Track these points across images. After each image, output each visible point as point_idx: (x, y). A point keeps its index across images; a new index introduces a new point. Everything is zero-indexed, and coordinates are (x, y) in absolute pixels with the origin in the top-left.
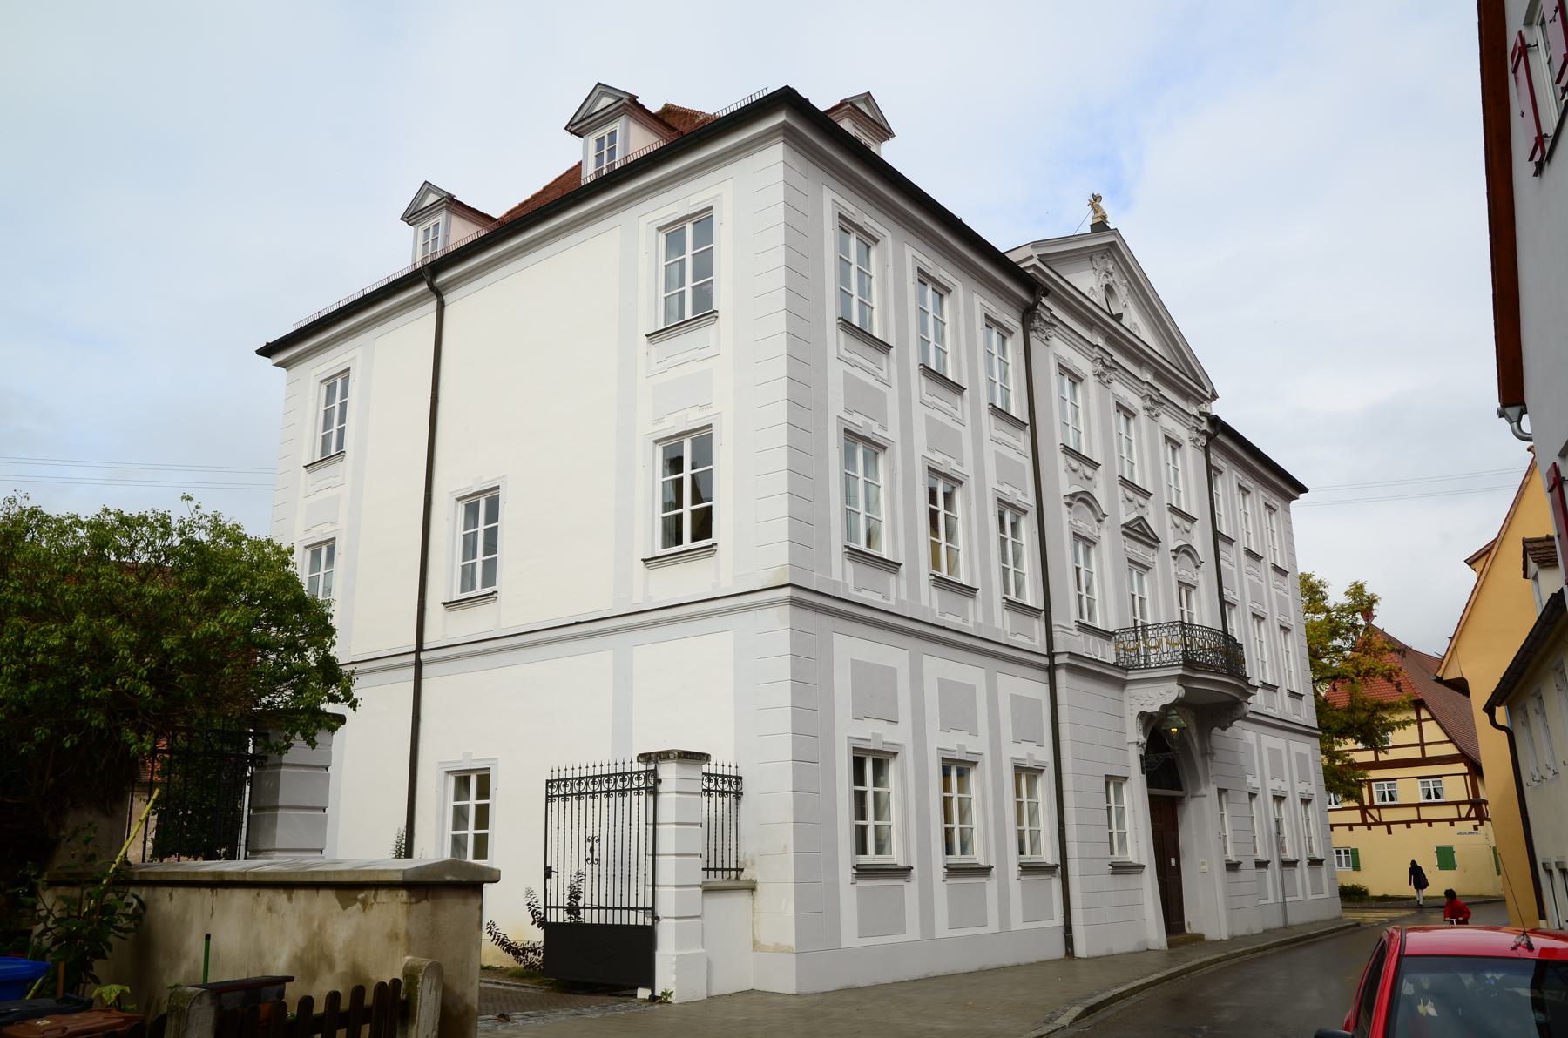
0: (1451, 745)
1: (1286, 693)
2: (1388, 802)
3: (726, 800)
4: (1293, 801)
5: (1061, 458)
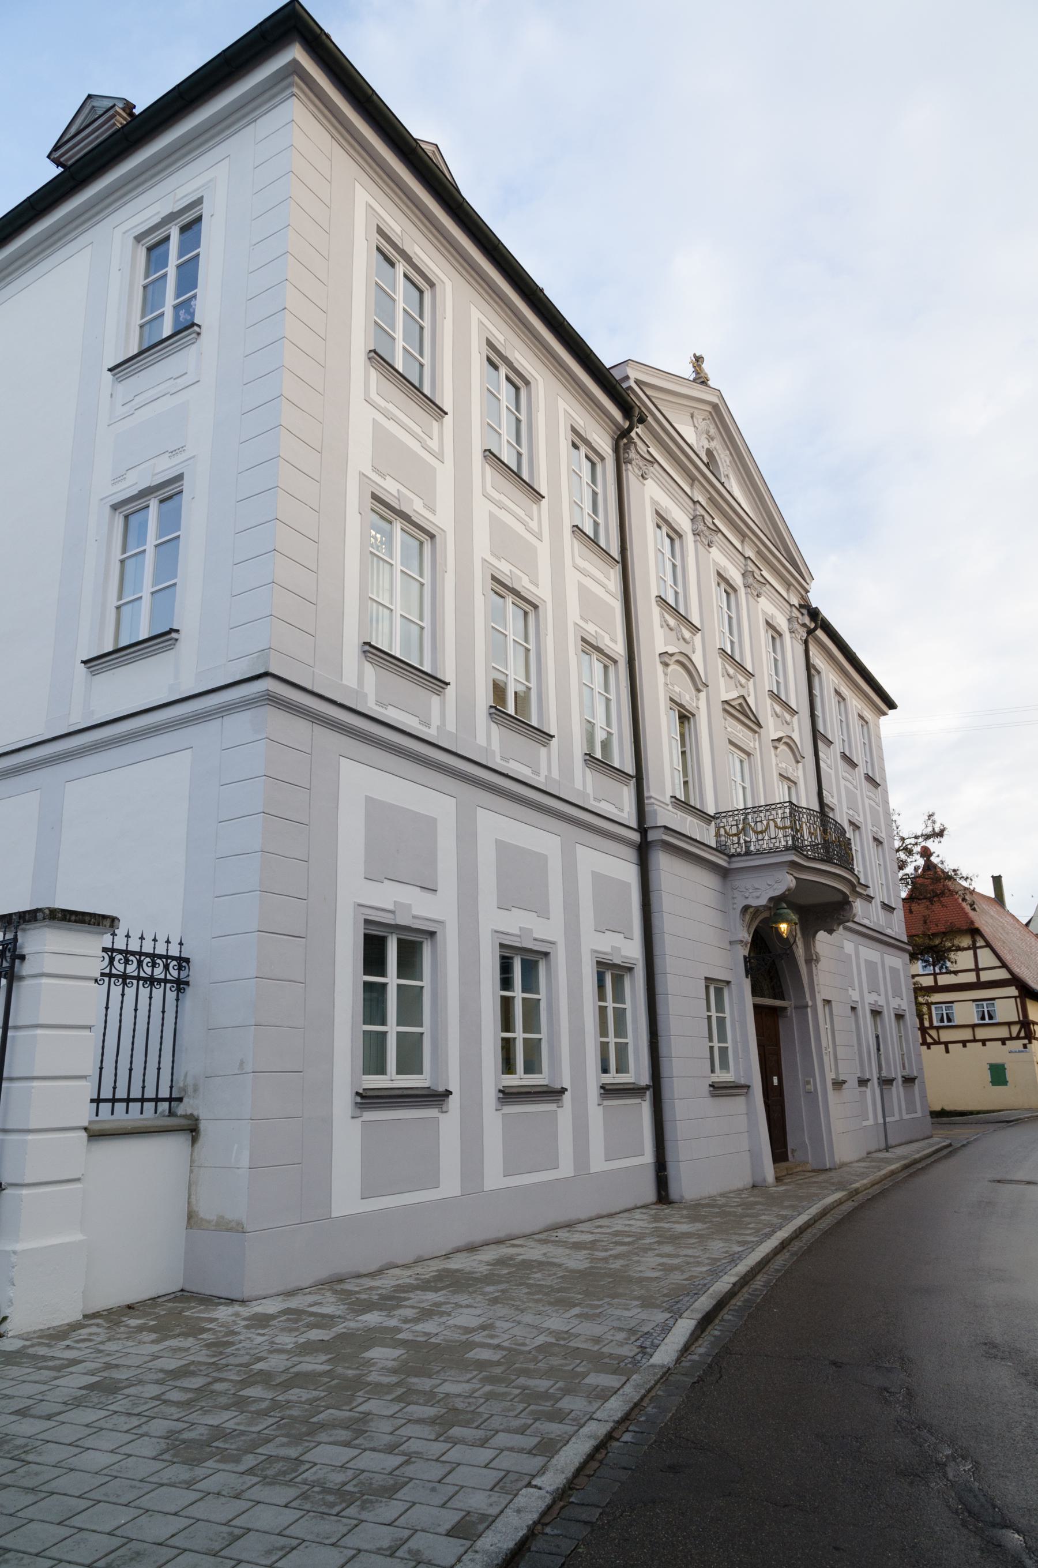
0: (1004, 970)
1: (879, 904)
2: (946, 1023)
3: (158, 993)
4: (889, 1017)
5: (656, 610)
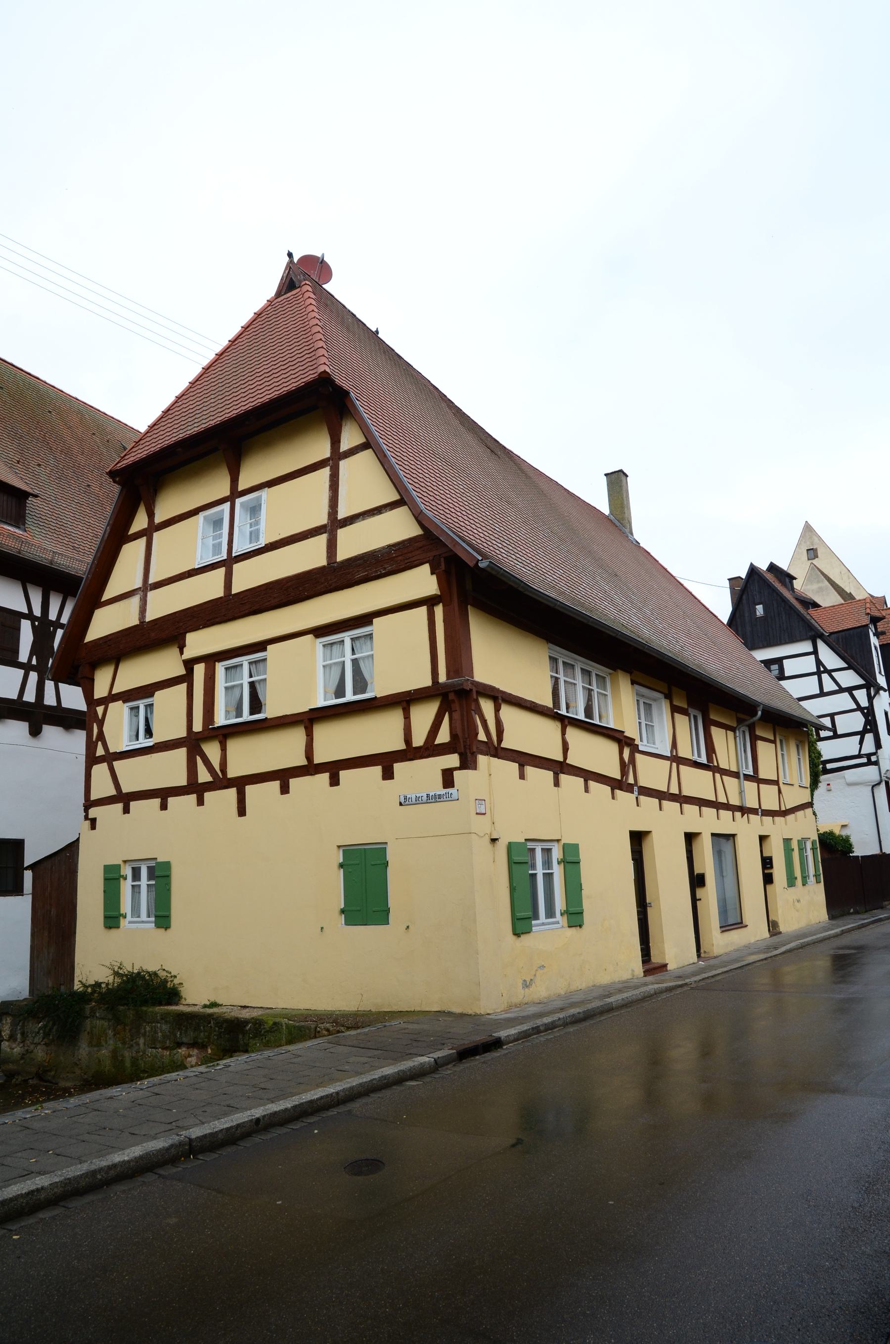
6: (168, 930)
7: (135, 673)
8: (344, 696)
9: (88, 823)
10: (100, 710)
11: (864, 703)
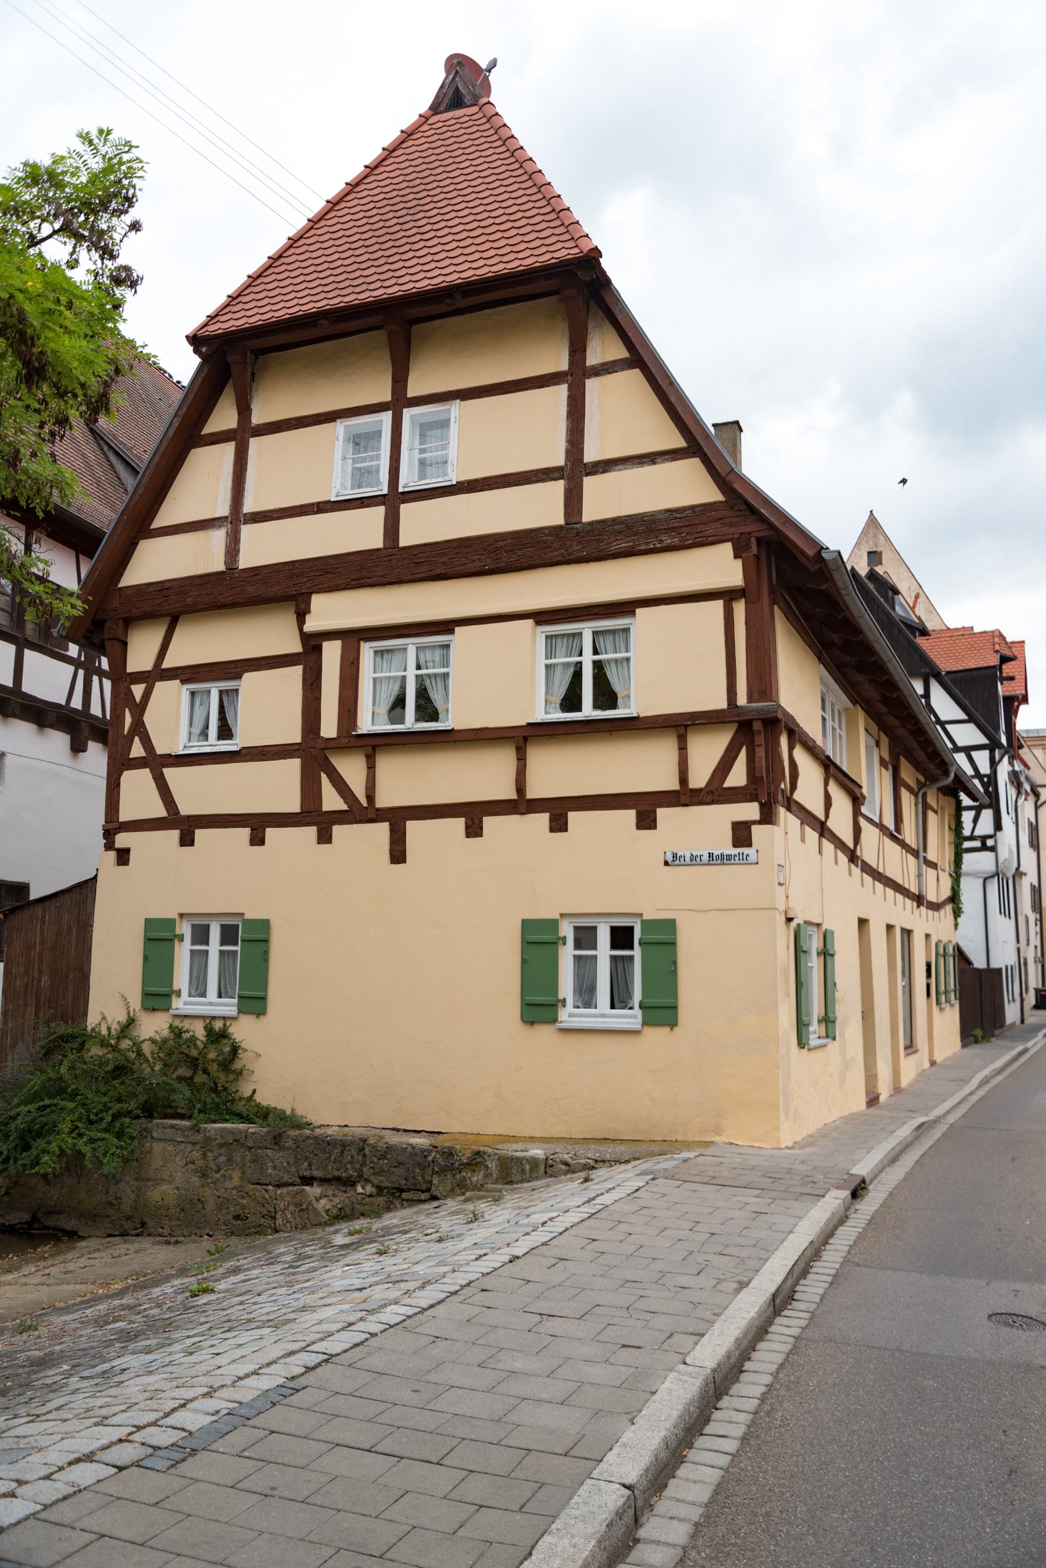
0: (693, 466)
2: (410, 722)
6: (262, 1018)
7: (198, 643)
8: (580, 710)
9: (112, 854)
10: (138, 690)
11: (985, 769)
